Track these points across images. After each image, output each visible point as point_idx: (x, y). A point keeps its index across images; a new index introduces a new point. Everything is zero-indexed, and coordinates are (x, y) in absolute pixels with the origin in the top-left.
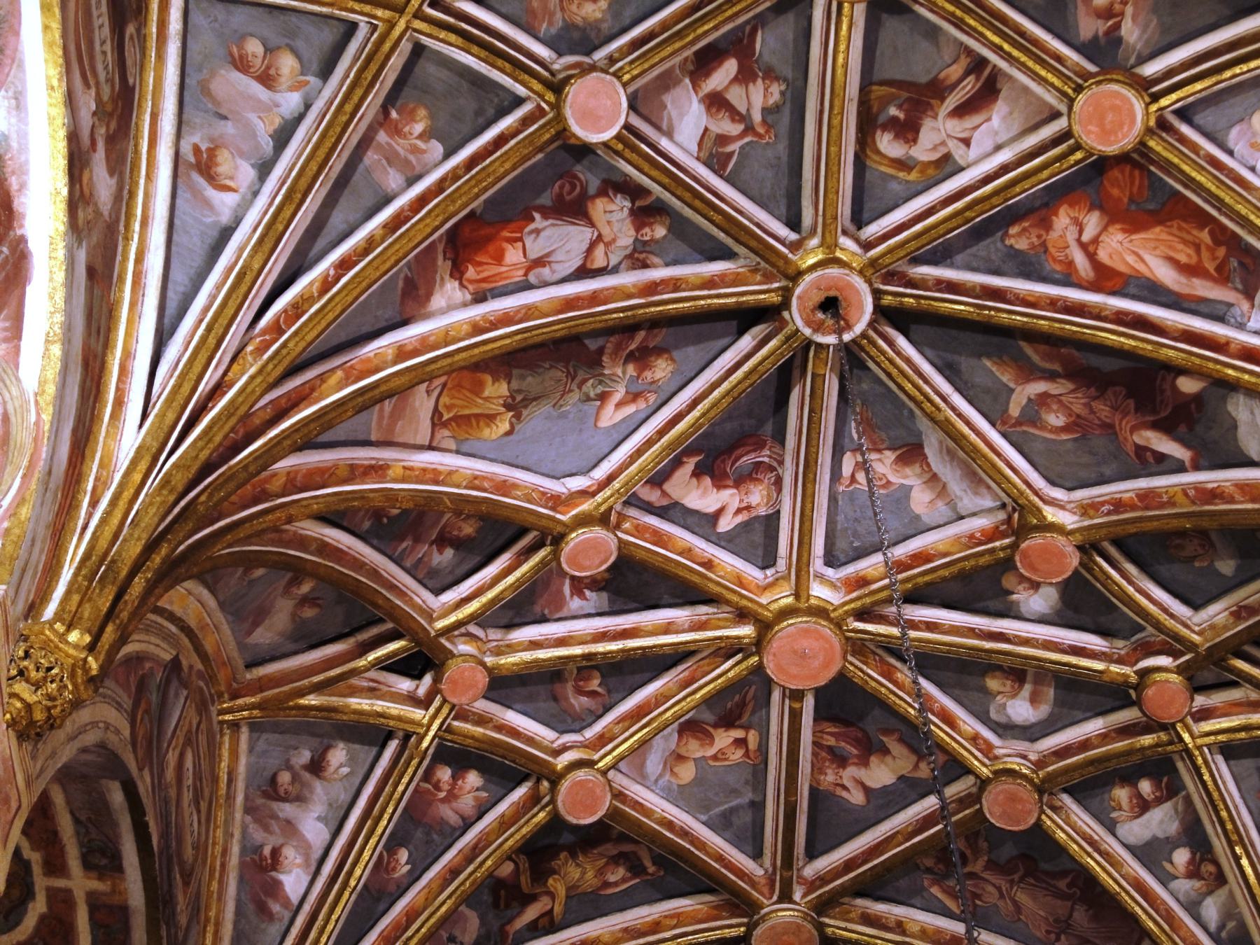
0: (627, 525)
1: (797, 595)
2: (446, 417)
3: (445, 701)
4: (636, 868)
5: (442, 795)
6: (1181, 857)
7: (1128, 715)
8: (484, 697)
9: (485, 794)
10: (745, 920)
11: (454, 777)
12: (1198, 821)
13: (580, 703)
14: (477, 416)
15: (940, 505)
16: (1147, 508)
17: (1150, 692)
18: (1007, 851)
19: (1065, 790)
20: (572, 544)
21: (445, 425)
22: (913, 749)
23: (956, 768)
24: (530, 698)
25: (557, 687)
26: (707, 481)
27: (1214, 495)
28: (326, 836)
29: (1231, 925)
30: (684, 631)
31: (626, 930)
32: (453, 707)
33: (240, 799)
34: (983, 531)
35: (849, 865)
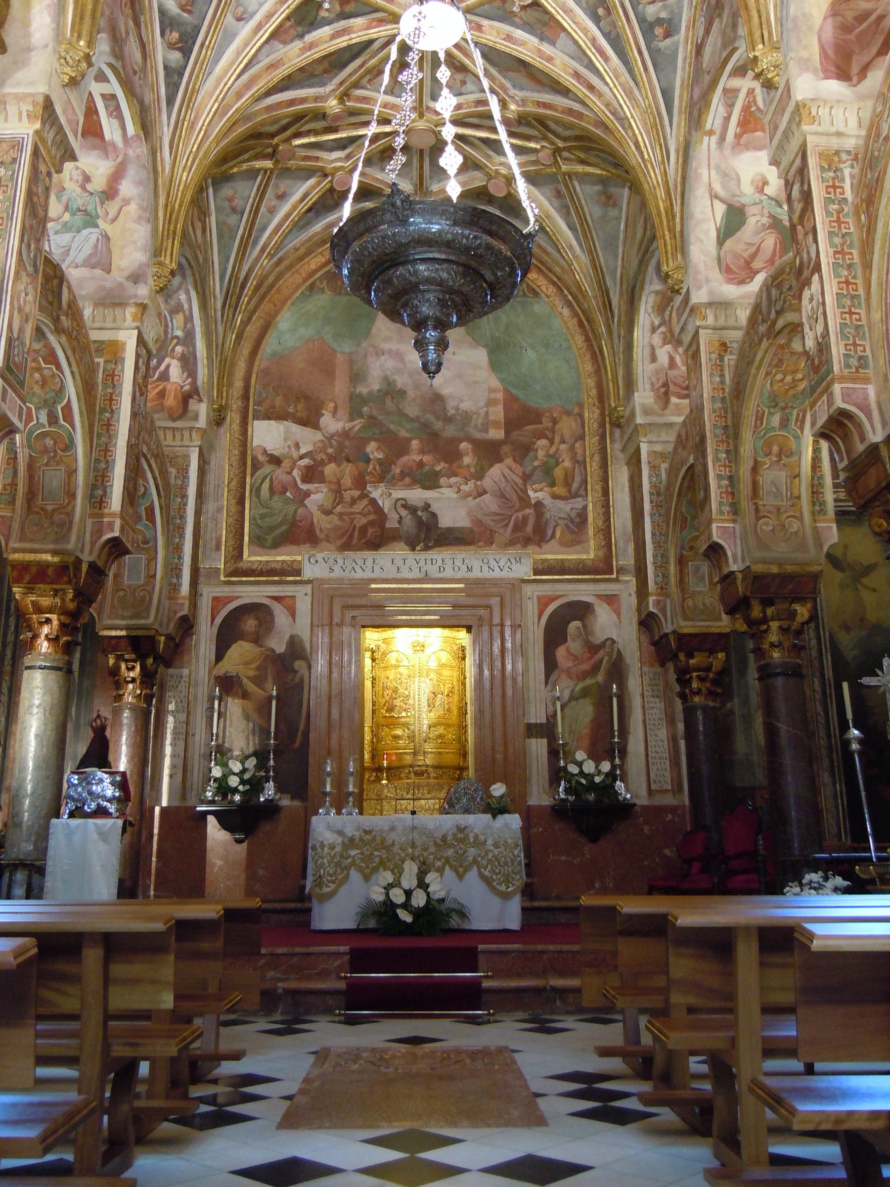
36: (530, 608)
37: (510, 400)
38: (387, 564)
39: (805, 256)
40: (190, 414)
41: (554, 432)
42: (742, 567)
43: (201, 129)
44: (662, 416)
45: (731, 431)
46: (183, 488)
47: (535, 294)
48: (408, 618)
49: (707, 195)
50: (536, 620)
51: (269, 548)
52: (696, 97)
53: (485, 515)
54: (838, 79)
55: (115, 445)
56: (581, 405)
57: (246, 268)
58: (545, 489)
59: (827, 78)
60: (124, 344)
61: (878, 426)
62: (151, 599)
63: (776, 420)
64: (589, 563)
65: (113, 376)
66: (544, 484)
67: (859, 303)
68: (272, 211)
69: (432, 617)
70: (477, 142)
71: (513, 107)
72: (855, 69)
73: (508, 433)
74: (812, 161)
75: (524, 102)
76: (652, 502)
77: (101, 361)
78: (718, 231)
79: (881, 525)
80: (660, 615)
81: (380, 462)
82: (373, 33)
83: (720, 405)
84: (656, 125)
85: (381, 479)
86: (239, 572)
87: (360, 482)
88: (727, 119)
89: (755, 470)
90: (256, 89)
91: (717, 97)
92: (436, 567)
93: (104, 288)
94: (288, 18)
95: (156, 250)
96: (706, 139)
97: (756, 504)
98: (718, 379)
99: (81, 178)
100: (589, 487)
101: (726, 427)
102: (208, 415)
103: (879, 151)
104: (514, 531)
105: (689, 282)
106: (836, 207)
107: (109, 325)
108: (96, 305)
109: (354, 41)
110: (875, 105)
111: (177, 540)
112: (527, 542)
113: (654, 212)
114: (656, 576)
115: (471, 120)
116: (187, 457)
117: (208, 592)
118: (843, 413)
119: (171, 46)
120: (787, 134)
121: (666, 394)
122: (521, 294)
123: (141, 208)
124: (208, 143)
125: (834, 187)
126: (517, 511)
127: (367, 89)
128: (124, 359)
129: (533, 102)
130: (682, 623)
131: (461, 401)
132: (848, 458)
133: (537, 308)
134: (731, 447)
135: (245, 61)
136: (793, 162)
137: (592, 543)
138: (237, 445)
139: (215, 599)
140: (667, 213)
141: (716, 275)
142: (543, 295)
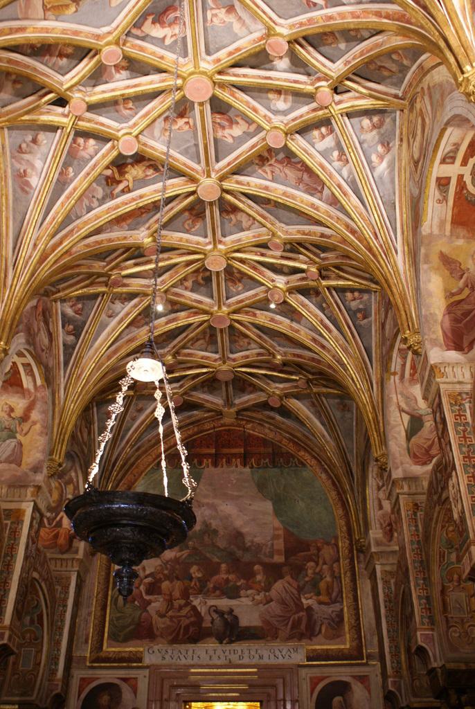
0: (128, 45)
1: (195, 68)
2: (48, 7)
3: (73, 115)
4: (156, 169)
5: (81, 148)
6: (336, 154)
7: (314, 105)
8: (87, 111)
9: (97, 147)
10: (196, 185)
11: (84, 142)
12: (340, 141)
13: (127, 112)
14: (61, 6)
15: (244, 28)
16: (310, 25)
17: (318, 95)
18: (281, 156)
19: (297, 132)
20: (104, 53)
21: (49, 10)
22: (247, 122)
23: (260, 129)
24: (107, 112)
25: (117, 107)
26: (158, 25)
27: (331, 18)
28: (42, 164)
29: (351, 176)
30: (157, 83)
31: (155, 191)
32: (76, 117)
33: (8, 153)
34: (258, 39)
35: (229, 164)
36: (305, 686)
37: (288, 535)
38: (203, 655)
40: (73, 549)
41: (318, 558)
42: (440, 665)
43: (84, 379)
44: (389, 546)
45: (425, 564)
46: (65, 600)
47: (304, 465)
48: (217, 695)
49: (397, 410)
50: (309, 696)
51: (121, 642)
52: (384, 353)
53: (272, 617)
54: (456, 350)
55: (11, 579)
56: (336, 538)
57: (116, 454)
58: (315, 598)
60: (24, 511)
62: (35, 681)
63: (453, 557)
64: (346, 651)
65: (15, 532)
66: (312, 594)
68: (134, 419)
69: (234, 694)
70: (261, 376)
71: (279, 357)
72: (466, 344)
73: (286, 558)
74: (444, 400)
75: (285, 354)
76: (386, 607)
77: (9, 522)
78: (406, 431)
80: (397, 693)
81: (199, 579)
82: (191, 320)
83: (417, 546)
84: (363, 368)
85: (200, 591)
86: (100, 659)
87: (185, 594)
88: (404, 365)
89: (443, 592)
90: (118, 354)
91: (395, 353)
92: (237, 656)
93: (15, 476)
94: (139, 314)
95: (50, 452)
96: (392, 377)
97: (446, 617)
98: (414, 528)
99: (8, 410)
100: (344, 596)
101: (421, 562)
102: (85, 549)
104: (292, 628)
105: (390, 465)
106: (461, 428)
107: (16, 499)
108: (10, 486)
109: (179, 325)
111: (58, 637)
112: (301, 637)
113: (366, 420)
114: (392, 662)
115: (256, 364)
116: (69, 579)
117: (78, 674)
119: (69, 333)
120: (429, 383)
121: (391, 530)
122: (294, 464)
123: (42, 426)
124: (88, 386)
125: (459, 415)
126: (294, 614)
127: (191, 349)
128: (23, 521)
129: (291, 354)
130: (413, 700)
131: (255, 537)
133: (304, 473)
134: (426, 576)
135: (112, 339)
137: (348, 636)
138: (104, 569)
139: (83, 680)
140: (374, 420)
141: (407, 459)
142: (308, 466)
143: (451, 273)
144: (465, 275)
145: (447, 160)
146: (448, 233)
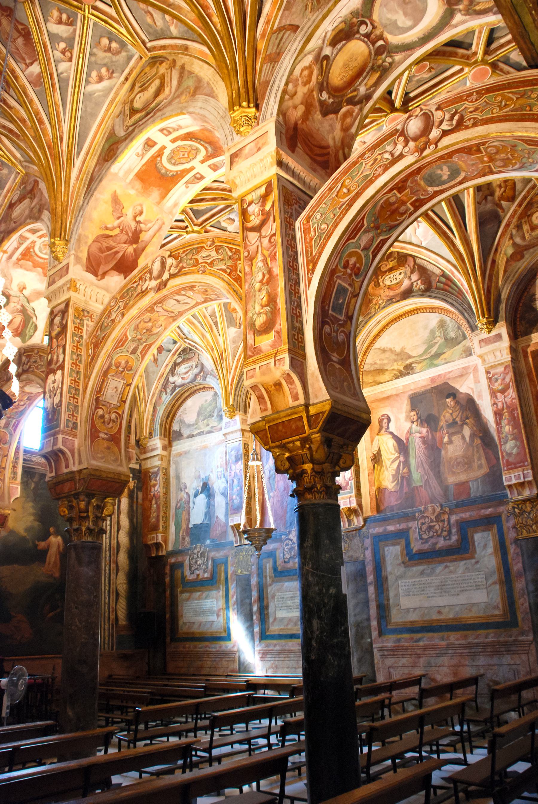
39: (55, 357)
59: (87, 271)
61: (77, 462)
67: (79, 394)
72: (100, 272)
74: (71, 311)
79: (64, 512)
88: (16, 249)
103: (108, 324)
110: (111, 300)
118: (61, 451)
120: (60, 289)
132: (56, 473)
136: (59, 304)
143: (113, 211)
144: (122, 219)
145: (165, 132)
146: (128, 180)
